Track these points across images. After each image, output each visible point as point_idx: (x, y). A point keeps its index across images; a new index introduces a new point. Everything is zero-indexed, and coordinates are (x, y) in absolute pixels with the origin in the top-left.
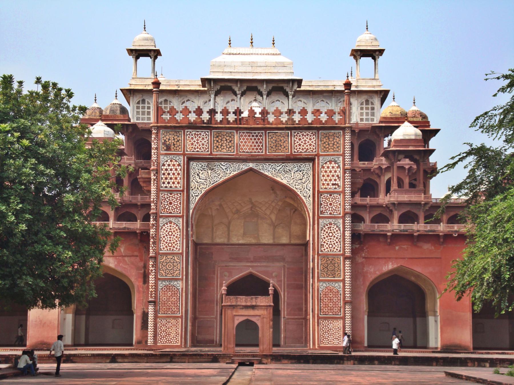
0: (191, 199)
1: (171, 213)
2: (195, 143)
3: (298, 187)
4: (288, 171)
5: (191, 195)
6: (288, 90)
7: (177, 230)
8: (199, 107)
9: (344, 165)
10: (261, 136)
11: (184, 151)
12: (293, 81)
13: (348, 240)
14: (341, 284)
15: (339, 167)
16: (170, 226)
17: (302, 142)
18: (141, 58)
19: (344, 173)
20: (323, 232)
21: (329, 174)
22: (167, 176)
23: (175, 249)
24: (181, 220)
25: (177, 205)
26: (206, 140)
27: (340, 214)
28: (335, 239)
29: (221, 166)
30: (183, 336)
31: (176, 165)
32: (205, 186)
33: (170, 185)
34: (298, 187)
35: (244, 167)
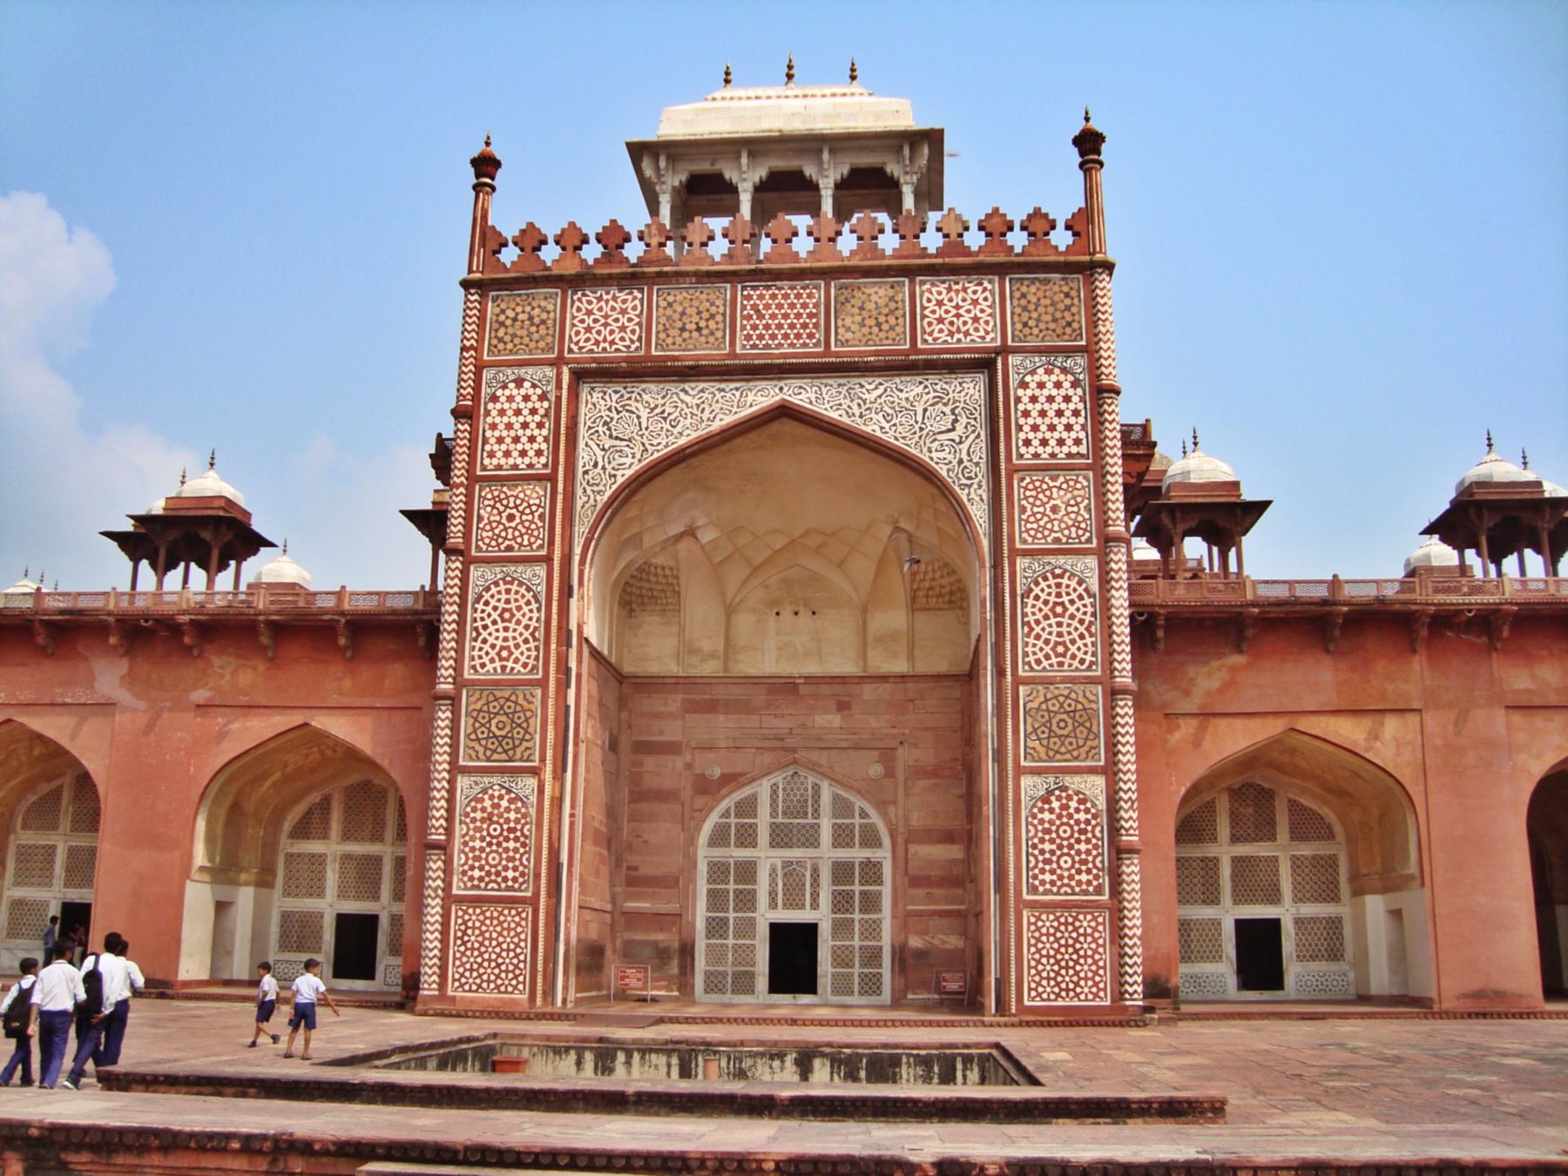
0: (579, 503)
1: (510, 548)
3: (941, 455)
4: (904, 403)
5: (579, 492)
7: (528, 603)
8: (613, 222)
10: (810, 296)
11: (561, 351)
13: (1122, 630)
14: (1100, 781)
15: (1075, 384)
16: (508, 591)
17: (947, 312)
20: (1030, 601)
21: (1046, 406)
22: (505, 433)
24: (541, 570)
25: (532, 522)
27: (1089, 541)
28: (1075, 623)
29: (682, 395)
30: (540, 967)
31: (534, 398)
32: (628, 461)
33: (511, 461)
34: (941, 455)
35: (761, 397)
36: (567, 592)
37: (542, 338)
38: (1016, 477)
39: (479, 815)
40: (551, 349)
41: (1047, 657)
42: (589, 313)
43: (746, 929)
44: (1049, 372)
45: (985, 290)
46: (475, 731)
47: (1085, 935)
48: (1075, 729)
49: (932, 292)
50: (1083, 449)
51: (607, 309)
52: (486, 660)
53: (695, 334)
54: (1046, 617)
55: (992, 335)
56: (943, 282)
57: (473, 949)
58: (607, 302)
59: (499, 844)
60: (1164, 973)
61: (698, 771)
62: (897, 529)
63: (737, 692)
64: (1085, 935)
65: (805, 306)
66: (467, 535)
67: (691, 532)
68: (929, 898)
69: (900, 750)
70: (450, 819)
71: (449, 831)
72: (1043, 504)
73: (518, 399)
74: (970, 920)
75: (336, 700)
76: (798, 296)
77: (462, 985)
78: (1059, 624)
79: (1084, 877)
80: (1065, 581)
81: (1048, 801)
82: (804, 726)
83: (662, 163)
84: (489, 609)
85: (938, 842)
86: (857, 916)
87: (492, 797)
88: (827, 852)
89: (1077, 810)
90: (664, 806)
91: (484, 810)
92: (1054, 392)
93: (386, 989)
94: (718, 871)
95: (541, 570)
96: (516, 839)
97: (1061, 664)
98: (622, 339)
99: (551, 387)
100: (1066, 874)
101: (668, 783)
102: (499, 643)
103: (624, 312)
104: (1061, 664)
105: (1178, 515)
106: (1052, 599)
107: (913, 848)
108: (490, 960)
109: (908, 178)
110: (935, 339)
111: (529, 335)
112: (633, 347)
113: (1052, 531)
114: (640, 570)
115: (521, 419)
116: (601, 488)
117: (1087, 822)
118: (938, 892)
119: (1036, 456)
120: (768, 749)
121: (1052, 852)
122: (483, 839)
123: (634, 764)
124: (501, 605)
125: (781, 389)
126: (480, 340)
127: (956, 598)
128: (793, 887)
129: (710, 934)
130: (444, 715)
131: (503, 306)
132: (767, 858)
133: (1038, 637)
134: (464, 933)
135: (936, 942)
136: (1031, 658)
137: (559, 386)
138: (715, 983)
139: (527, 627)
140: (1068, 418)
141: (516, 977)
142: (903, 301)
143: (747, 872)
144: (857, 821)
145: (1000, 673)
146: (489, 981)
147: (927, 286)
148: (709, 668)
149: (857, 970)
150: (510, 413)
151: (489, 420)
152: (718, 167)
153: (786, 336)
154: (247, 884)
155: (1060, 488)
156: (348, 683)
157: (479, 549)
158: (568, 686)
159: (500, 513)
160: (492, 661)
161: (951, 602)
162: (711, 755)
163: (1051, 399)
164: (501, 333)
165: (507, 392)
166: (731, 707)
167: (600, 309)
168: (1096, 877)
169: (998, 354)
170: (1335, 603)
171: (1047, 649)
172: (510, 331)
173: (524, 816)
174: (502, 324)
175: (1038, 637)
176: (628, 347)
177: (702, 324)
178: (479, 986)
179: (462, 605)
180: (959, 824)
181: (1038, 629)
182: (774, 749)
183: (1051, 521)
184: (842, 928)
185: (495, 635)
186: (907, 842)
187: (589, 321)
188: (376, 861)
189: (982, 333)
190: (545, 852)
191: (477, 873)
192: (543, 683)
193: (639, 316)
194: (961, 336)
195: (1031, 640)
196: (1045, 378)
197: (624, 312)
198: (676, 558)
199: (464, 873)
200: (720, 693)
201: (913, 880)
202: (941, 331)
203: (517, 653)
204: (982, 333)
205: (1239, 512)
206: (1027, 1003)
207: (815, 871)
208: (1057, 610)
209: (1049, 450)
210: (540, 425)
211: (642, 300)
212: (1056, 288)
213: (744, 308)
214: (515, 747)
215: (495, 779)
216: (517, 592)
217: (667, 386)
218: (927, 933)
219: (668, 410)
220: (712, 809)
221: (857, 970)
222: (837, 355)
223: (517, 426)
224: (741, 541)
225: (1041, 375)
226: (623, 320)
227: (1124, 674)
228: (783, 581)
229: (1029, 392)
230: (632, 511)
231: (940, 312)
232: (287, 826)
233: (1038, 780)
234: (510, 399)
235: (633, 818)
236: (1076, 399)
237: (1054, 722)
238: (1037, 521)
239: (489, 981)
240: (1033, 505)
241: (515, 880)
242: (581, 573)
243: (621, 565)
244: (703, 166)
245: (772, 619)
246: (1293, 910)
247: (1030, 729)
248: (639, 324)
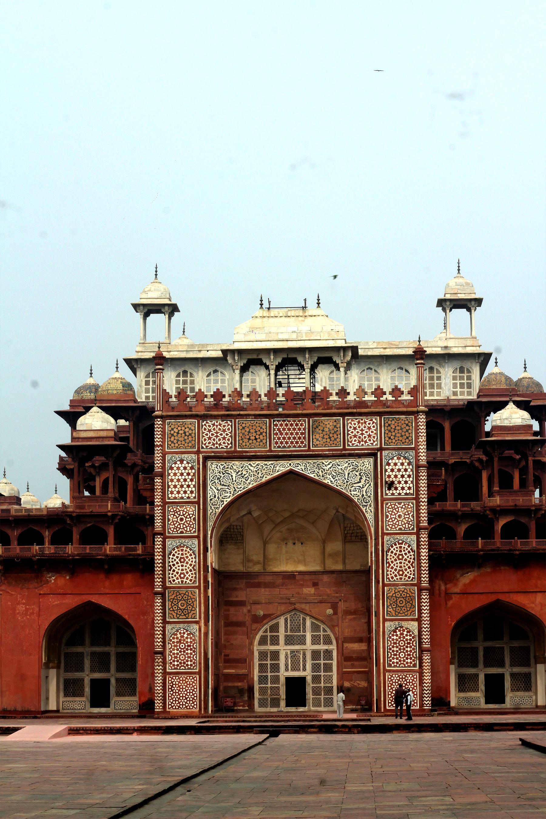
0: (209, 513)
1: (182, 532)
2: (213, 437)
3: (355, 493)
4: (340, 471)
5: (209, 508)
6: (338, 361)
7: (191, 555)
9: (417, 460)
10: (302, 425)
11: (199, 448)
12: (345, 349)
13: (425, 564)
14: (416, 624)
17: (358, 432)
18: (153, 317)
19: (417, 472)
20: (389, 554)
21: (397, 473)
23: (188, 581)
24: (196, 542)
25: (190, 521)
26: (228, 432)
27: (413, 529)
28: (407, 562)
29: (249, 466)
31: (188, 468)
32: (228, 495)
33: (180, 495)
34: (355, 493)
35: (282, 467)
36: (206, 550)
37: (190, 442)
38: (384, 503)
39: (175, 640)
40: (194, 447)
41: (396, 576)
42: (210, 431)
43: (276, 679)
44: (399, 459)
45: (373, 422)
46: (172, 607)
47: (409, 682)
48: (406, 604)
49: (352, 423)
50: (411, 491)
51: (217, 429)
52: (175, 578)
53: (254, 441)
54: (395, 560)
55: (376, 442)
56: (356, 419)
57: (176, 693)
58: (217, 426)
59: (184, 652)
60: (444, 696)
61: (253, 614)
62: (337, 511)
63: (268, 579)
64: (409, 682)
65: (299, 429)
66: (164, 527)
67: (250, 513)
68: (353, 666)
69: (340, 603)
70: (164, 642)
71: (164, 646)
72: (395, 514)
73: (182, 468)
74: (368, 676)
75: (102, 590)
76: (297, 425)
77: (172, 707)
78: (401, 563)
79: (409, 661)
80: (403, 546)
81: (396, 632)
82: (298, 593)
83: (236, 358)
84: (175, 558)
85: (356, 642)
86: (322, 674)
87: (180, 633)
88: (309, 646)
89: (407, 635)
90: (239, 628)
91: (177, 638)
92: (401, 467)
93: (115, 711)
94: (263, 655)
95: (196, 542)
96: (191, 649)
97: (401, 579)
98: (224, 443)
99: (195, 464)
100: (402, 659)
101: (240, 619)
102: (180, 571)
103: (224, 431)
104: (401, 579)
105: (496, 446)
106: (398, 553)
107: (346, 645)
108: (183, 697)
109: (342, 364)
110: (353, 444)
111: (185, 440)
112: (229, 447)
113: (398, 525)
114: (227, 528)
115: (183, 477)
116: (218, 506)
117: (410, 640)
118: (356, 663)
119: (393, 494)
120: (283, 603)
121: (397, 651)
122: (177, 650)
123: (226, 610)
124: (180, 556)
125: (290, 464)
126: (163, 442)
127: (362, 538)
128: (295, 661)
129: (260, 683)
130: (158, 601)
131: (173, 427)
133: (392, 568)
134: (172, 686)
135: (356, 684)
136: (390, 576)
137: (199, 464)
138: (262, 704)
139: (191, 565)
140: (406, 478)
141: (193, 703)
142: (340, 427)
143: (275, 655)
144: (322, 633)
145: (377, 582)
146: (183, 705)
147: (350, 421)
148: (257, 568)
149: (322, 697)
150: (178, 474)
151: (170, 477)
152: (260, 357)
153: (292, 443)
154: (53, 668)
155: (402, 508)
156: (107, 584)
157: (169, 533)
158: (209, 588)
159: (177, 518)
160: (177, 579)
161: (361, 539)
162: (259, 606)
163: (399, 470)
164: (173, 438)
165: (177, 465)
166: (267, 585)
167: (214, 429)
168: (414, 661)
169: (378, 451)
170: (516, 550)
171: (396, 573)
172: (176, 438)
173: (194, 640)
174: (173, 435)
175: (392, 568)
176: (227, 447)
177: (257, 437)
178: (179, 707)
179: (164, 556)
180: (365, 635)
181: (392, 565)
182: (286, 603)
183: (398, 521)
184: (316, 679)
185: (178, 568)
186: (343, 642)
187: (209, 435)
188: (108, 654)
189: (372, 442)
190: (202, 654)
191: (176, 663)
192: (199, 587)
193: (231, 433)
194: (363, 443)
195: (390, 569)
196: (397, 461)
197: (224, 431)
198: (242, 522)
199: (171, 663)
200: (262, 579)
201: (345, 658)
202: (355, 441)
203: (187, 576)
204: (372, 442)
205: (530, 444)
206: (387, 708)
207: (304, 654)
208: (400, 557)
209: (398, 492)
210: (192, 480)
211: (232, 426)
212: (403, 422)
213: (274, 430)
214: (188, 613)
215: (181, 626)
216: (186, 551)
217: (243, 463)
218: (352, 680)
219: (244, 473)
220: (260, 630)
221: (322, 697)
222: (313, 451)
223: (182, 480)
224: (270, 515)
225: (395, 460)
226: (224, 434)
227: (425, 584)
228: (288, 529)
229: (390, 467)
230: (228, 512)
231: (355, 432)
232: (64, 641)
233: (392, 623)
234: (178, 468)
235: (226, 634)
236: (409, 470)
237: (398, 601)
238: (393, 521)
239: (183, 705)
240: (391, 514)
241: (191, 665)
242: (211, 541)
243: (222, 529)
244: (255, 357)
245: (284, 547)
246: (510, 670)
247: (388, 604)
248: (231, 436)
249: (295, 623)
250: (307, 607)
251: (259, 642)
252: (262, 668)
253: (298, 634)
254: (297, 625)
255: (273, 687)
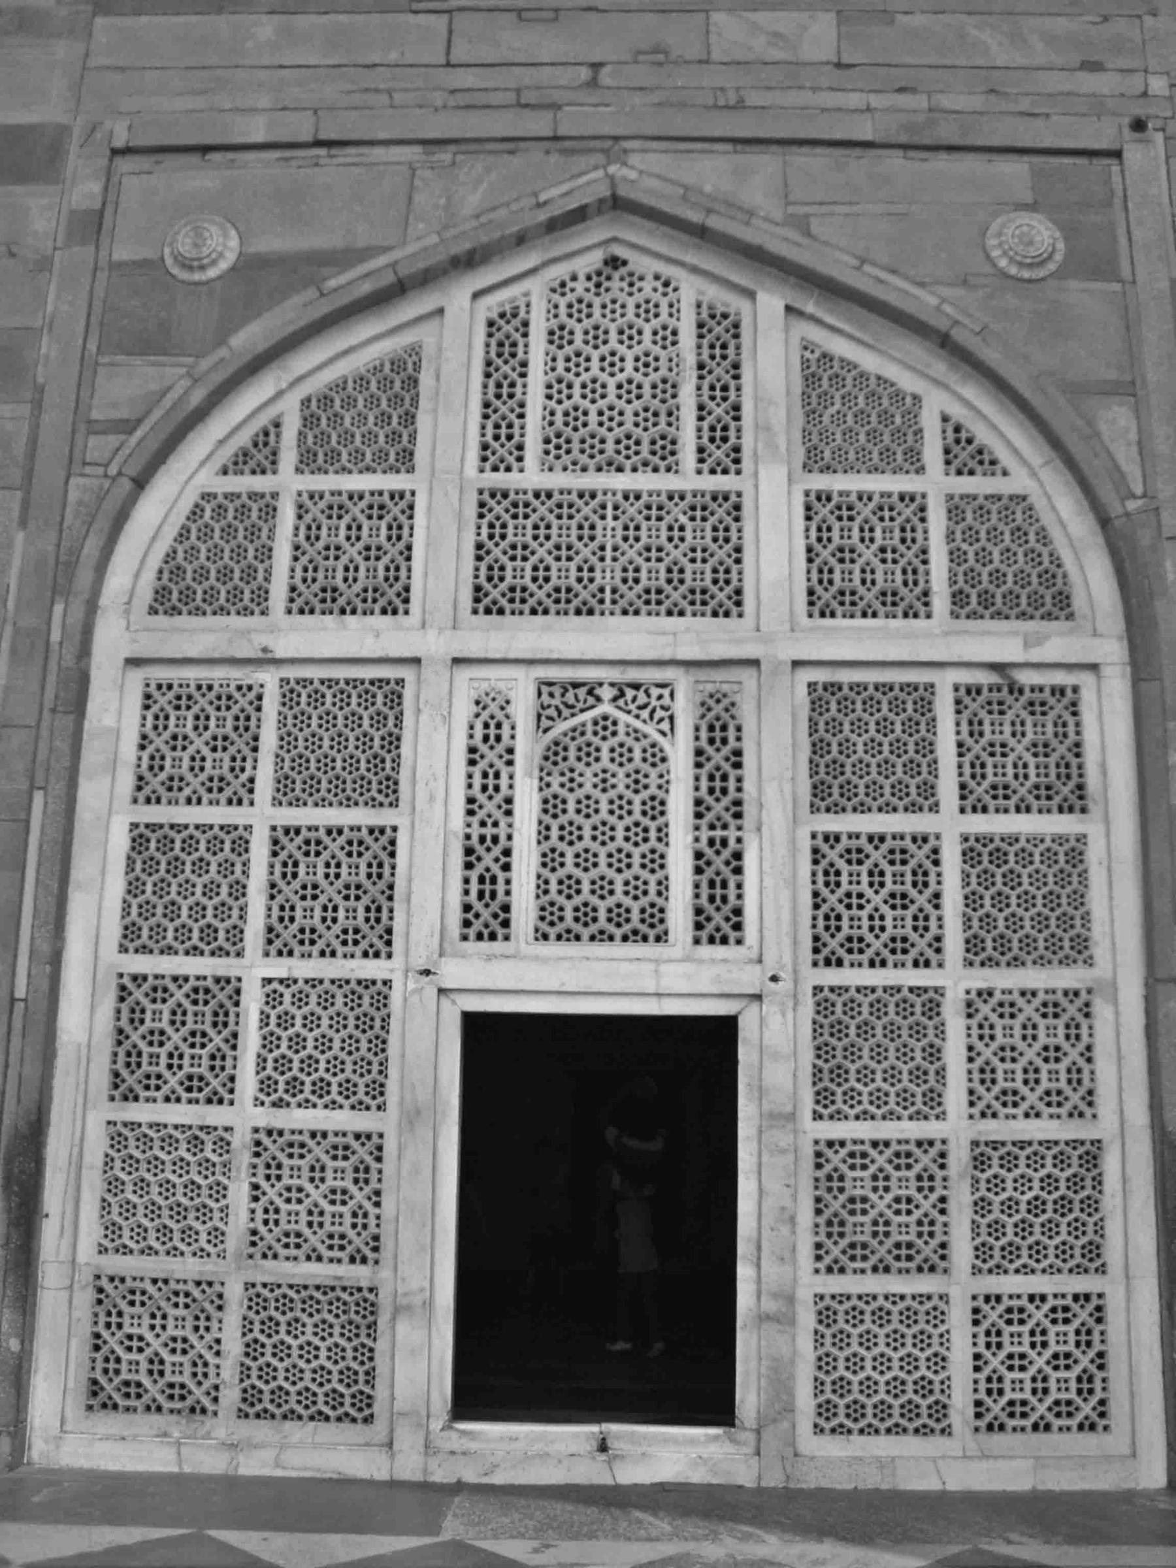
94: (195, 732)
132: (456, 666)
144: (935, 483)
149: (960, 1285)
207: (720, 734)
249: (611, 362)
250: (753, 191)
251: (172, 568)
252: (174, 880)
253: (644, 482)
254: (629, 390)
255: (296, 1146)
